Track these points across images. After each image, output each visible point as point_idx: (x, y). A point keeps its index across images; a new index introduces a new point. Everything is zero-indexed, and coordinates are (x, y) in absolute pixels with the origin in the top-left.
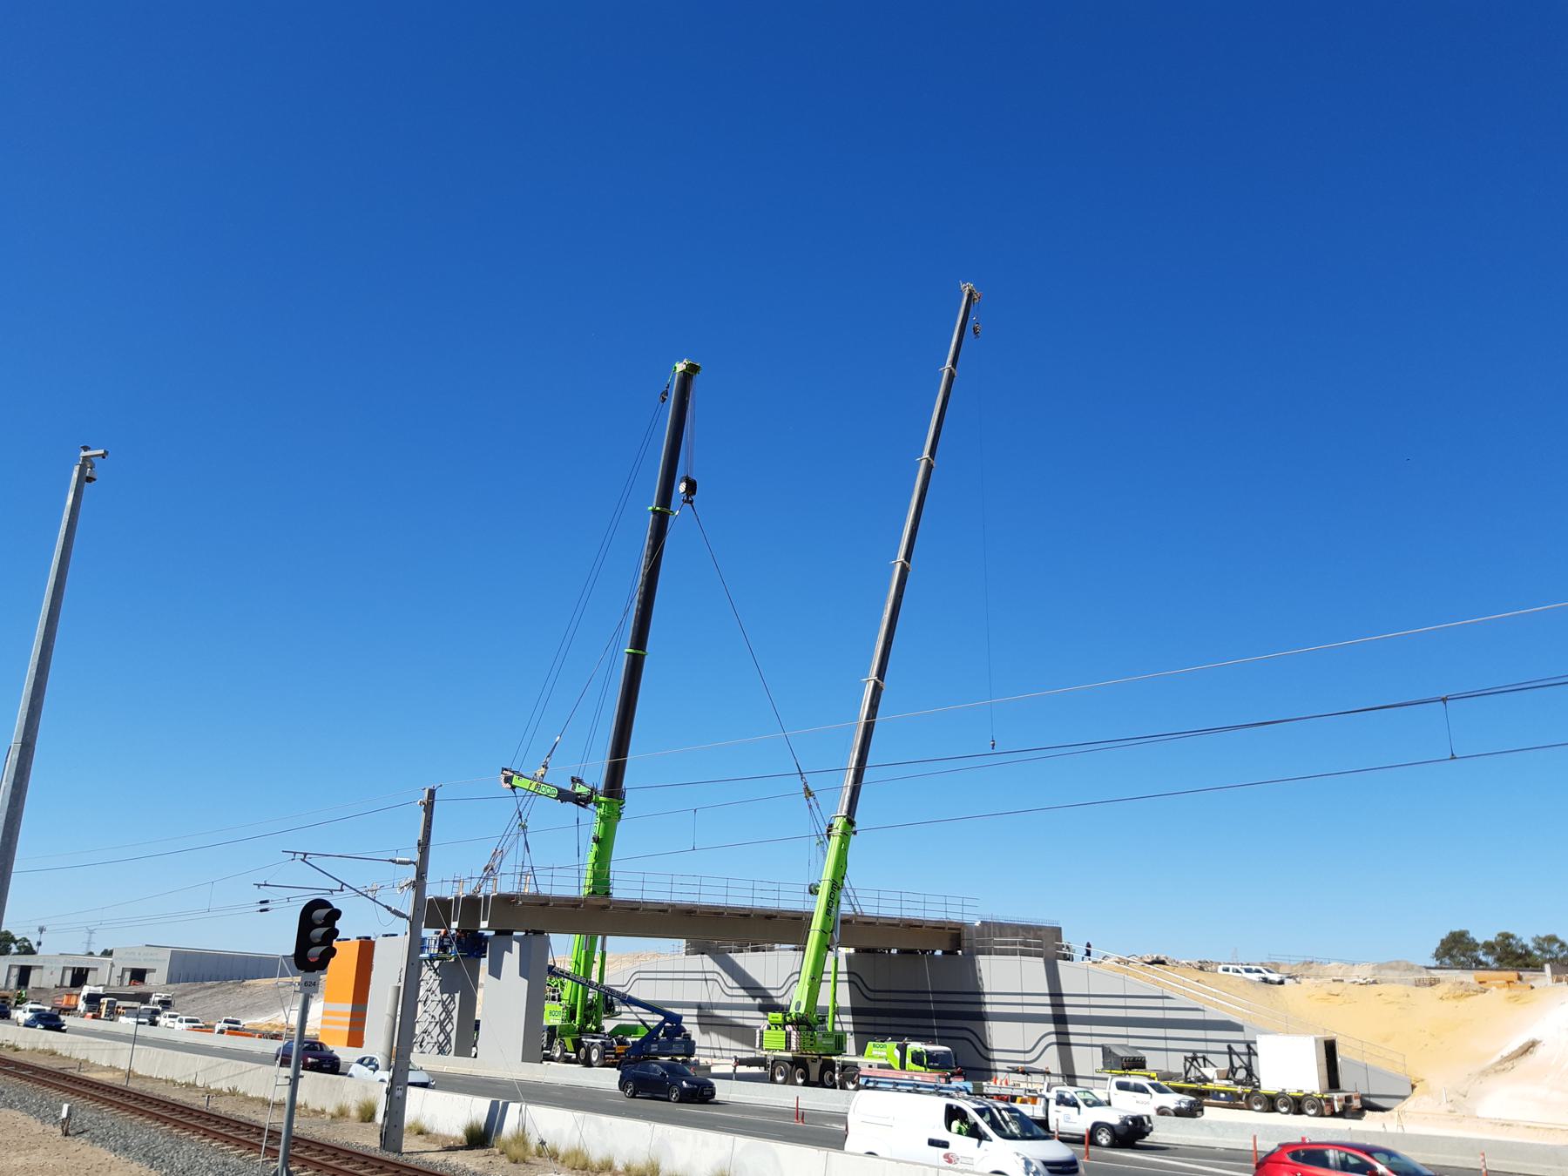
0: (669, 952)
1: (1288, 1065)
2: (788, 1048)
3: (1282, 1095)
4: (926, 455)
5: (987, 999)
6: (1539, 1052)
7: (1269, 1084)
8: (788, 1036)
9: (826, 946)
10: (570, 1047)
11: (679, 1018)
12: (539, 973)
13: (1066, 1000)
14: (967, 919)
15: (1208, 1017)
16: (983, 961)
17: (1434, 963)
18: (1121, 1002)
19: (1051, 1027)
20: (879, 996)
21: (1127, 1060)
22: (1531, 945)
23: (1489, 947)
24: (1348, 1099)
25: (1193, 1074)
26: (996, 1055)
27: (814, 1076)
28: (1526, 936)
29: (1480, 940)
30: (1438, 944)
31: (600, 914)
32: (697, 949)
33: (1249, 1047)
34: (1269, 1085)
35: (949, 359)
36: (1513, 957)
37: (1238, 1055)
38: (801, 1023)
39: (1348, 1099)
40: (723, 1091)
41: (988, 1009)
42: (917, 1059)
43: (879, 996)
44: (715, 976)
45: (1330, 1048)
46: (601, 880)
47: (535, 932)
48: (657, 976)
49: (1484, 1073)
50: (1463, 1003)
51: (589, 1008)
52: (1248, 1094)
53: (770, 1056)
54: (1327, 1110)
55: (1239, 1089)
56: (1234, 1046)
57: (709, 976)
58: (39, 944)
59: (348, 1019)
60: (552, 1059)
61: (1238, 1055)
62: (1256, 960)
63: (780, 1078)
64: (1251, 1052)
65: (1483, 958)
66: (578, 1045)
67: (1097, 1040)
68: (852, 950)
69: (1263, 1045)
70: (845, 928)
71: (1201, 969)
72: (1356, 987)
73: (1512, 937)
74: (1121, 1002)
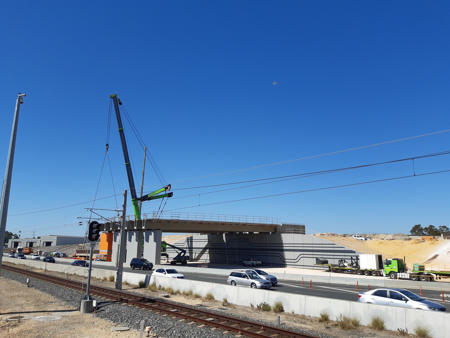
1: (368, 262)
3: (366, 270)
5: (284, 245)
6: (438, 258)
12: (157, 239)
14: (278, 224)
17: (411, 234)
18: (321, 246)
25: (341, 265)
26: (287, 261)
28: (437, 227)
33: (357, 257)
36: (433, 232)
37: (354, 259)
41: (284, 248)
54: (379, 274)
55: (354, 269)
58: (20, 236)
64: (358, 259)
69: (361, 257)
71: (344, 236)
73: (433, 227)
74: (321, 246)
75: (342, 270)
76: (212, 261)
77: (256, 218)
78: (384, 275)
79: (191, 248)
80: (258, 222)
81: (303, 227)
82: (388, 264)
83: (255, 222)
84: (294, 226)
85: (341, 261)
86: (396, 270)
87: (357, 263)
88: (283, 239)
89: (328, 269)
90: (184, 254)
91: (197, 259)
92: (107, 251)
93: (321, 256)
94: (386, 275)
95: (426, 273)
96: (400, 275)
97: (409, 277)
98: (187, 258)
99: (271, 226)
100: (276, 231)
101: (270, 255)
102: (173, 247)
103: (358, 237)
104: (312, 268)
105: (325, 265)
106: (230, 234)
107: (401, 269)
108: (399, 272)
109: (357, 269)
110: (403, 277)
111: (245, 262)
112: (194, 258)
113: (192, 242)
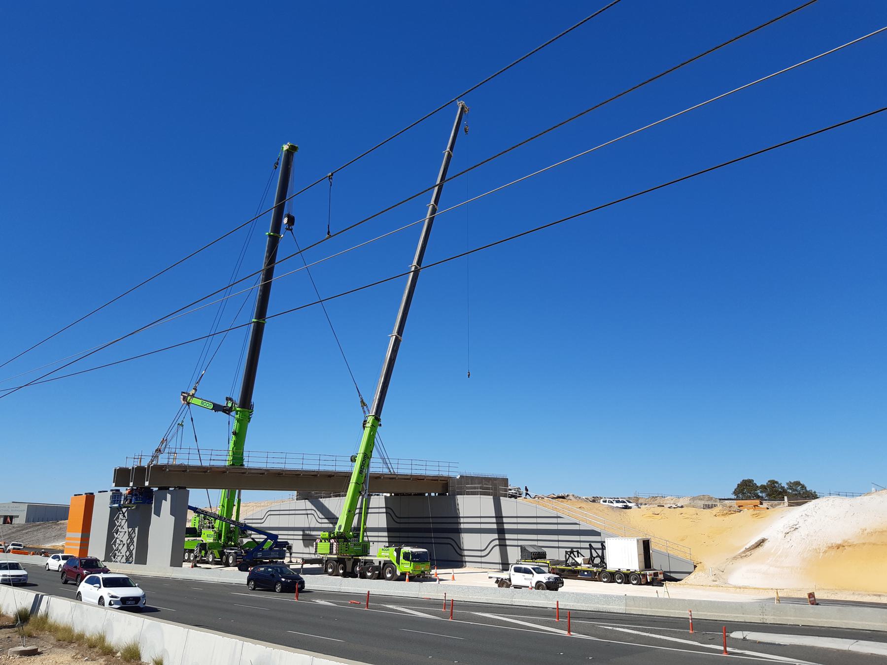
0: (287, 499)
1: (622, 555)
2: (331, 553)
4: (432, 202)
5: (462, 520)
6: (766, 545)
7: (612, 565)
8: (332, 545)
9: (358, 492)
10: (217, 555)
11: (276, 536)
12: (180, 510)
13: (505, 520)
14: (452, 475)
16: (460, 498)
17: (733, 497)
18: (534, 520)
19: (496, 536)
20: (402, 520)
22: (786, 487)
23: (764, 488)
24: (656, 574)
25: (570, 561)
26: (466, 553)
27: (349, 569)
29: (759, 485)
31: (236, 477)
32: (302, 497)
33: (603, 545)
34: (612, 566)
35: (449, 146)
36: (774, 493)
37: (595, 549)
38: (341, 538)
39: (656, 574)
40: (311, 582)
41: (462, 526)
42: (406, 556)
43: (402, 520)
44: (313, 512)
45: (646, 545)
46: (238, 456)
47: (180, 488)
48: (280, 513)
49: (735, 558)
50: (728, 518)
51: (229, 531)
52: (600, 572)
53: (325, 558)
54: (643, 581)
55: (595, 569)
56: (594, 545)
57: (309, 512)
59: (79, 542)
60: (207, 563)
62: (621, 496)
63: (330, 570)
64: (603, 548)
65: (760, 494)
66: (222, 554)
67: (520, 543)
68: (388, 495)
69: (610, 543)
70: (373, 483)
71: (594, 501)
72: (672, 509)
73: (777, 482)
74: (534, 520)
77: (432, 463)
80: (408, 472)
84: (485, 478)
85: (571, 552)
87: (602, 558)
88: (461, 507)
93: (532, 542)
99: (435, 480)
109: (600, 570)
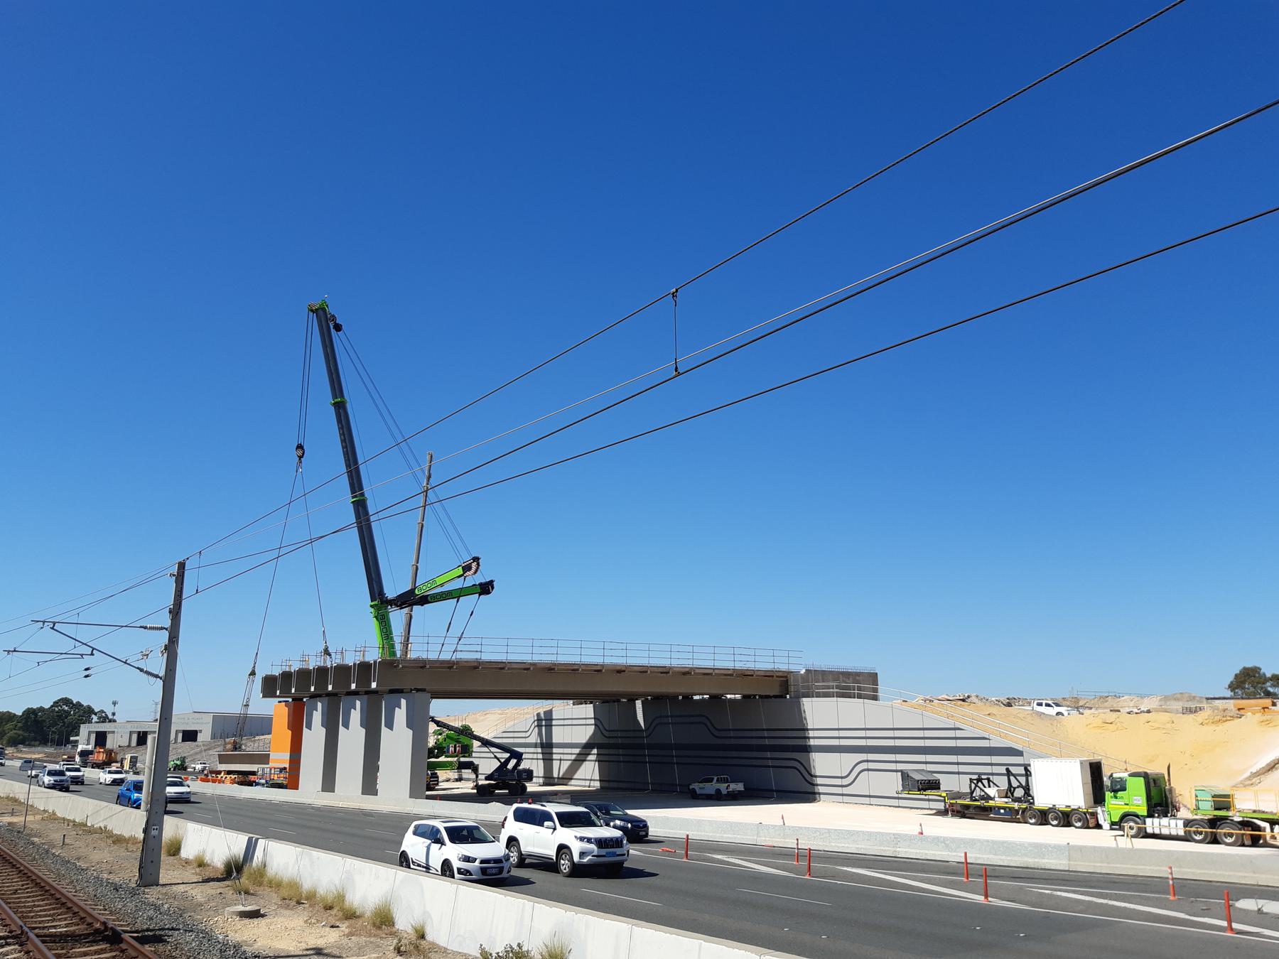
1: (1059, 784)
5: (811, 734)
14: (793, 668)
15: (993, 744)
16: (808, 704)
21: (921, 782)
25: (977, 793)
26: (819, 781)
30: (1231, 678)
33: (1026, 770)
37: (1015, 776)
41: (812, 742)
55: (1016, 805)
56: (1011, 768)
61: (1015, 776)
64: (1028, 773)
69: (1037, 767)
71: (1009, 705)
75: (979, 810)
76: (606, 785)
78: (1106, 826)
79: (547, 747)
80: (730, 665)
81: (873, 678)
82: (1115, 791)
83: (719, 665)
84: (843, 673)
86: (1143, 811)
87: (1027, 789)
89: (941, 806)
90: (518, 764)
91: (565, 779)
92: (287, 756)
93: (919, 766)
94: (1113, 824)
95: (1237, 819)
96: (1152, 825)
97: (1181, 833)
98: (524, 776)
99: (769, 676)
100: (782, 690)
101: (770, 763)
102: (486, 743)
103: (1048, 705)
104: (895, 802)
105: (931, 794)
106: (655, 702)
107: (1156, 805)
108: (1150, 815)
109: (1024, 806)
110: (1165, 831)
111: (695, 786)
112: (555, 775)
113: (549, 727)
